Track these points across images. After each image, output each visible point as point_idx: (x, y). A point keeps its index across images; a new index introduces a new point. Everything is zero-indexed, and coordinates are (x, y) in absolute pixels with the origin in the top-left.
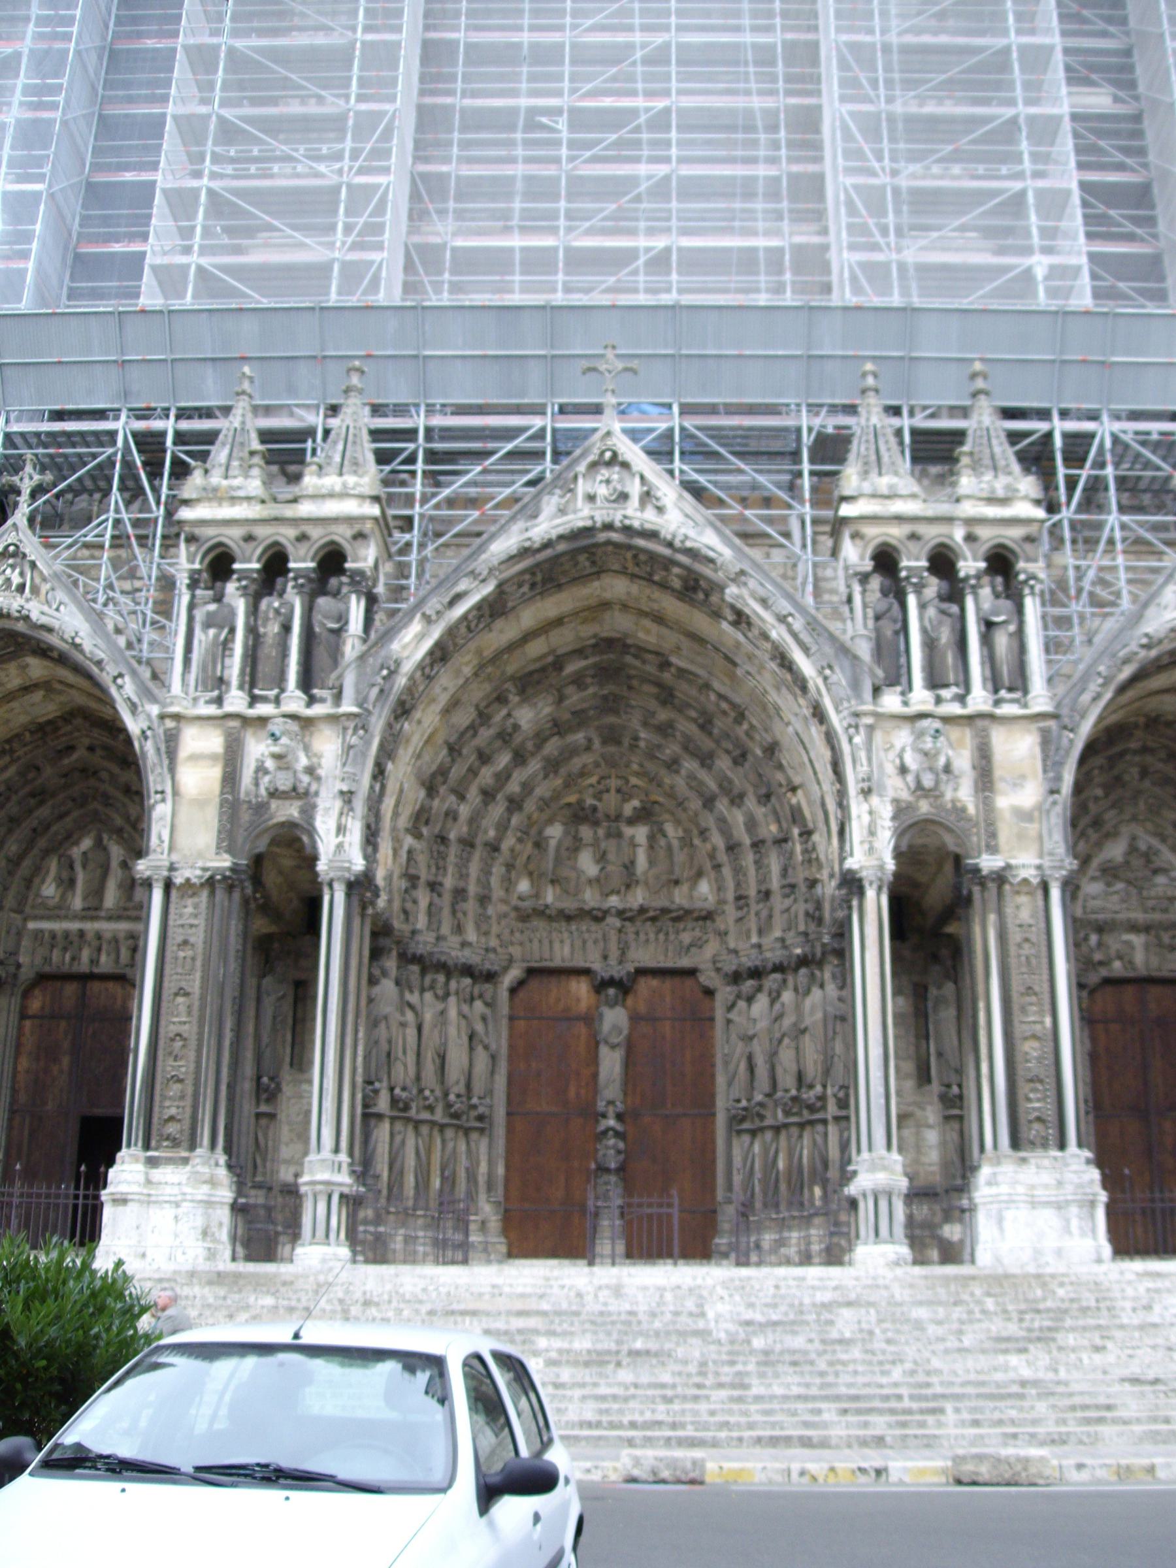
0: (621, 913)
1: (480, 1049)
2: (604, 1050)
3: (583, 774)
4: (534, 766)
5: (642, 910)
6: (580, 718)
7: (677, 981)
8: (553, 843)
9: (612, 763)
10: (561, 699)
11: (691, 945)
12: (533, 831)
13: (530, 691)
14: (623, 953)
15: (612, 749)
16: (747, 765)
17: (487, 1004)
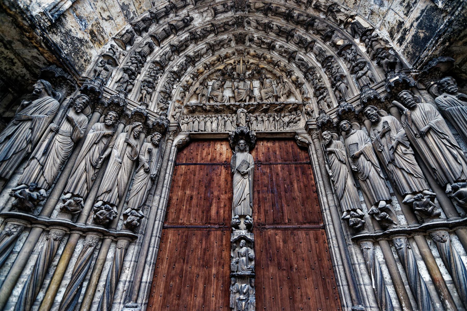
0: (247, 107)
1: (142, 171)
2: (237, 177)
3: (226, 57)
4: (202, 46)
5: (259, 104)
6: (225, 27)
7: (283, 143)
8: (210, 87)
9: (240, 53)
10: (216, 13)
11: (289, 123)
12: (201, 78)
13: (198, 4)
14: (248, 122)
15: (241, 48)
16: (316, 24)
17: (156, 146)
